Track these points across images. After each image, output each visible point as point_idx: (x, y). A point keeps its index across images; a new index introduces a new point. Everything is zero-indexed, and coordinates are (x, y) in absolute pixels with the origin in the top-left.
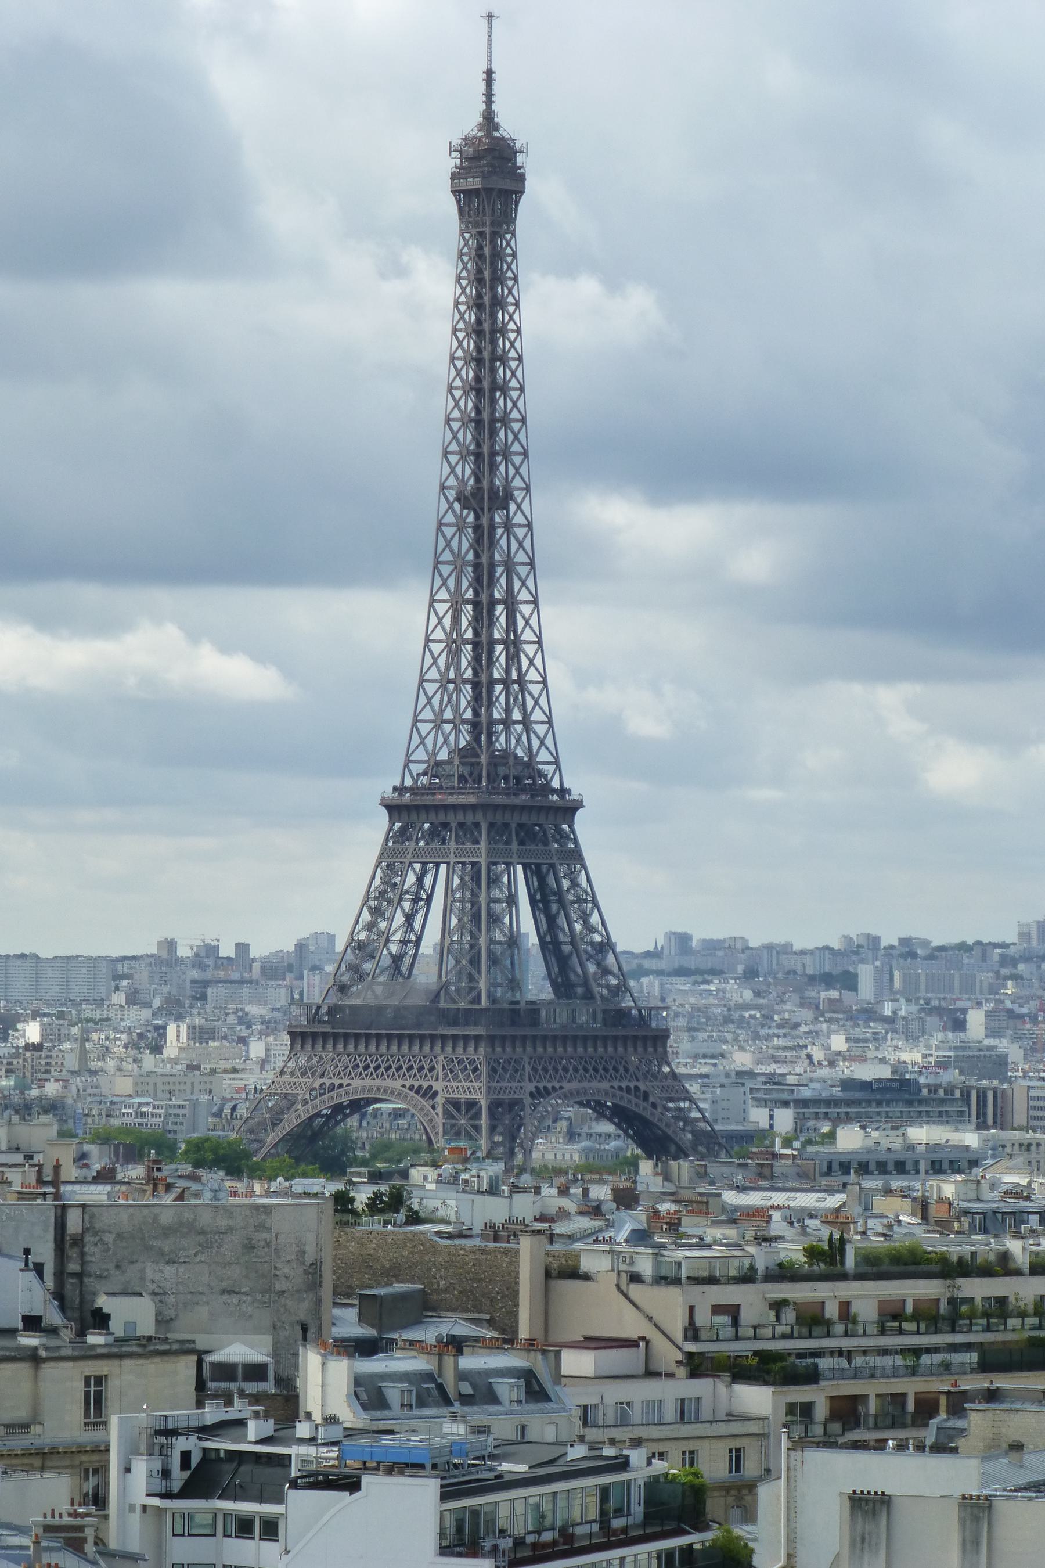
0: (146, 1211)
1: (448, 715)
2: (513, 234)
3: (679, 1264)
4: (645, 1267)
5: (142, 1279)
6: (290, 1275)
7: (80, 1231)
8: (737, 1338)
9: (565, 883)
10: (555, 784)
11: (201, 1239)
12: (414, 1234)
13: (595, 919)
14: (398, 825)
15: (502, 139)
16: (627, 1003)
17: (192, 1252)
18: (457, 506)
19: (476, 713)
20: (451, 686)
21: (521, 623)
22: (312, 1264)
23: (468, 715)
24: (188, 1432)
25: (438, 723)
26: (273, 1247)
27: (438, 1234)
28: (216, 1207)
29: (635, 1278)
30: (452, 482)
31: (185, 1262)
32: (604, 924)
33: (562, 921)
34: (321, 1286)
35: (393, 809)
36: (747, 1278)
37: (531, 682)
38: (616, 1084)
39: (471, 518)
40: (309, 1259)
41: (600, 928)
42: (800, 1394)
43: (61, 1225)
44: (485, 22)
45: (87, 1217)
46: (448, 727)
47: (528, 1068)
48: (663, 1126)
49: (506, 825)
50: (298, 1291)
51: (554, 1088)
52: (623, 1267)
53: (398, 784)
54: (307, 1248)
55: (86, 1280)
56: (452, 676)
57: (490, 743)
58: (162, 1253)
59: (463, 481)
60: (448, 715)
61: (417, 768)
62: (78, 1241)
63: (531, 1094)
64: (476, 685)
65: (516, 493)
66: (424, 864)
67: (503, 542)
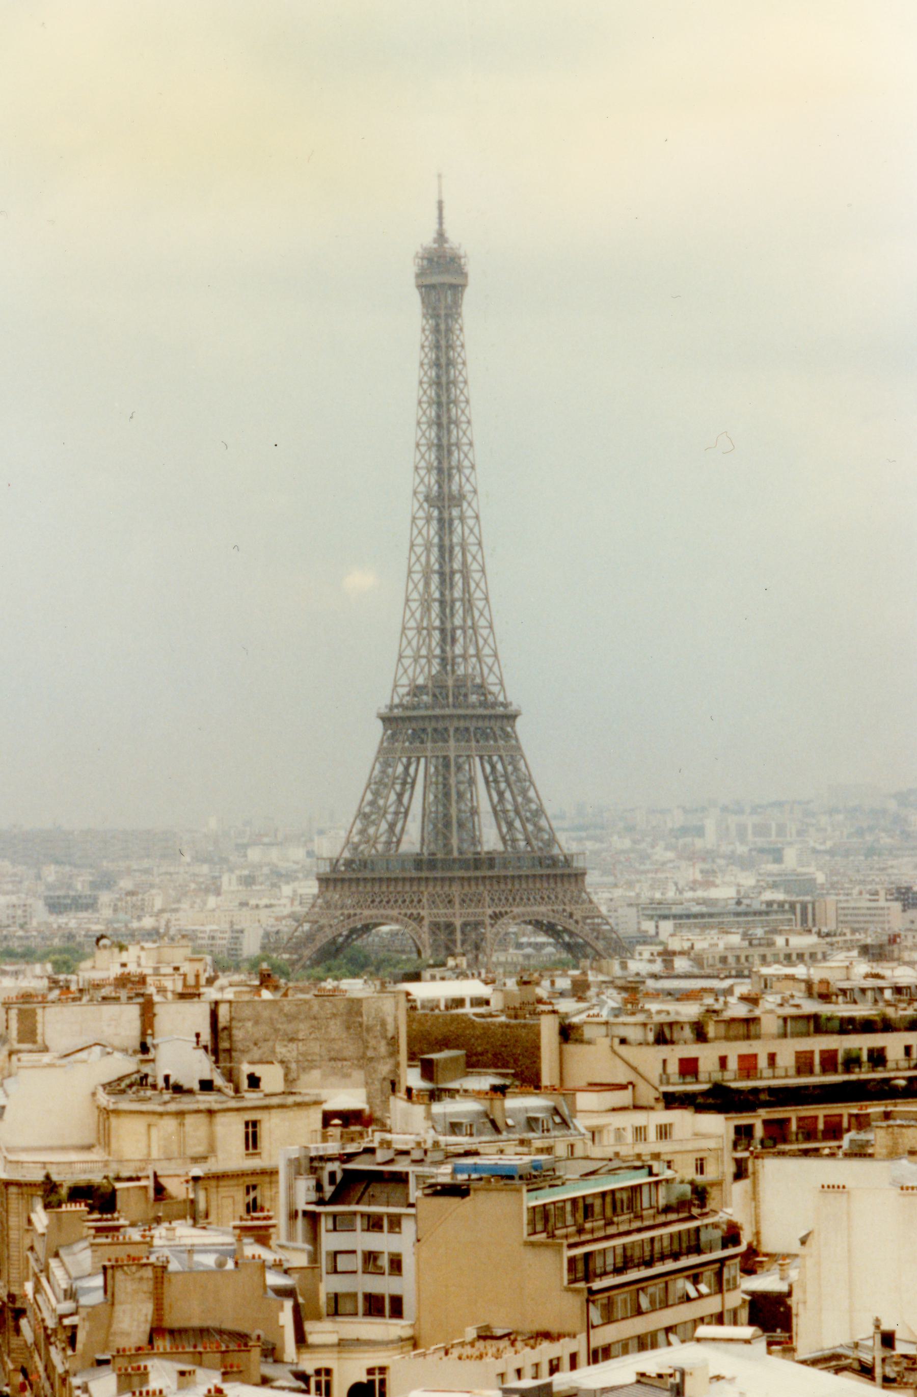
2: (459, 315)
5: (273, 1052)
8: (774, 1077)
9: (510, 768)
11: (314, 1022)
12: (458, 1015)
13: (531, 794)
14: (389, 732)
16: (555, 851)
18: (426, 505)
20: (425, 632)
23: (437, 651)
27: (476, 1015)
29: (623, 1041)
30: (422, 488)
33: (508, 795)
35: (387, 720)
37: (482, 627)
38: (550, 907)
39: (436, 513)
40: (390, 1035)
41: (536, 799)
42: (744, 1119)
43: (214, 1016)
46: (423, 661)
47: (488, 899)
49: (467, 729)
51: (506, 913)
53: (388, 702)
55: (234, 1054)
56: (425, 624)
57: (453, 671)
59: (429, 487)
60: (424, 652)
61: (403, 691)
63: (491, 917)
66: (409, 758)
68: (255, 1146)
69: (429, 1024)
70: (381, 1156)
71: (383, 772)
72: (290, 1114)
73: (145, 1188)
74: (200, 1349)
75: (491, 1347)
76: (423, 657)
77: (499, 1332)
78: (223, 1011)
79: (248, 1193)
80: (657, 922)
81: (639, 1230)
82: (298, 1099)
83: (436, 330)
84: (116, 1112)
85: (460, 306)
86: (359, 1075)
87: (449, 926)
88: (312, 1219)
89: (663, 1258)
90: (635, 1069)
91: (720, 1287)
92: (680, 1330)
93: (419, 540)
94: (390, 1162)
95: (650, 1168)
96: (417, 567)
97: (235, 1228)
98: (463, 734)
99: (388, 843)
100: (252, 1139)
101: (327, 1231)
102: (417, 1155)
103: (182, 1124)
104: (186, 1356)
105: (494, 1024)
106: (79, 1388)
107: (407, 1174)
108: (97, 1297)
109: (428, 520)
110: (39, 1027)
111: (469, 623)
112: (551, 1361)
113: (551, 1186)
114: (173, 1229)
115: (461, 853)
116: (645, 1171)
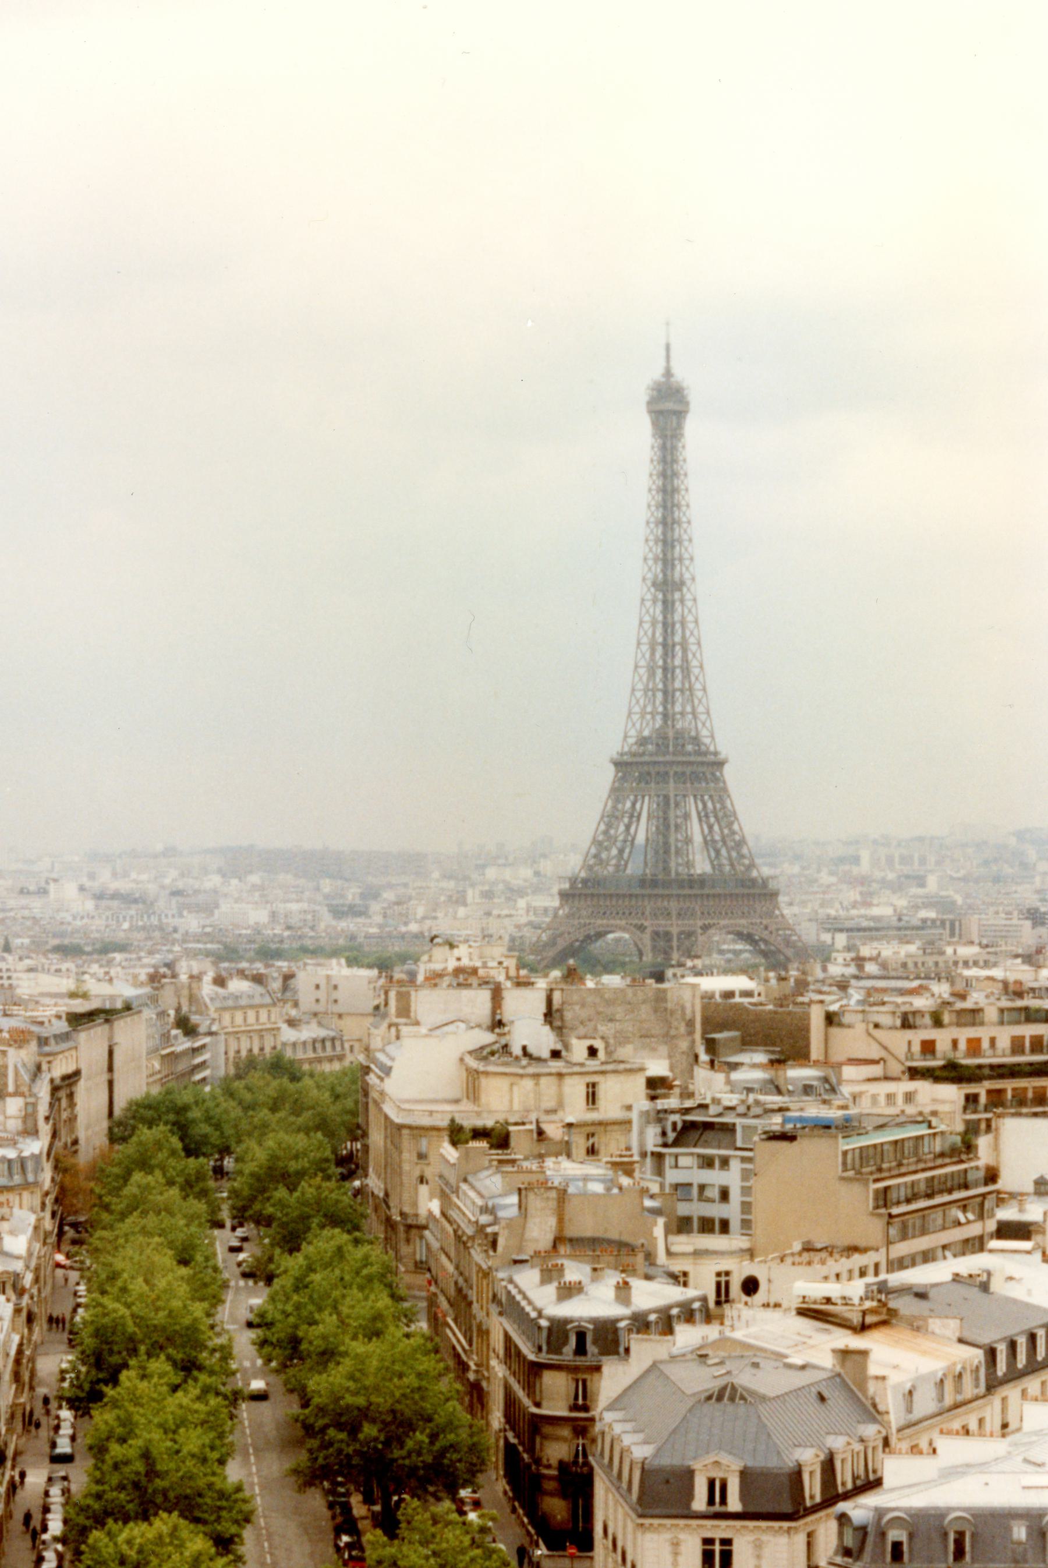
2: (682, 435)
5: (595, 1029)
9: (718, 806)
10: (712, 749)
13: (736, 827)
14: (620, 774)
18: (653, 590)
21: (690, 656)
23: (660, 709)
24: (673, 1112)
27: (751, 1004)
29: (876, 1026)
30: (650, 576)
32: (741, 829)
33: (716, 828)
35: (618, 764)
39: (660, 596)
40: (688, 1017)
46: (649, 717)
47: (699, 913)
53: (619, 749)
57: (673, 726)
59: (656, 576)
60: (649, 709)
61: (631, 741)
63: (701, 928)
64: (665, 692)
66: (636, 796)
68: (594, 1102)
70: (713, 1110)
71: (614, 807)
72: (622, 1078)
73: (531, 1131)
74: (598, 1253)
75: (816, 1257)
77: (819, 1246)
78: (557, 997)
79: (588, 1139)
81: (924, 1170)
82: (628, 1066)
83: (663, 448)
84: (487, 1074)
86: (664, 1049)
87: (667, 936)
88: (659, 1157)
89: (941, 1192)
90: (885, 1048)
91: (981, 1216)
92: (953, 1247)
93: (647, 618)
94: (720, 1115)
95: (930, 1122)
96: (645, 640)
97: (607, 1163)
98: (680, 777)
99: (617, 866)
100: (592, 1097)
101: (671, 1167)
102: (741, 1109)
103: (537, 1084)
104: (586, 1258)
106: (503, 1280)
107: (734, 1125)
108: (513, 1212)
109: (655, 601)
110: (413, 1005)
111: (687, 686)
112: (860, 1269)
113: (859, 1134)
114: (559, 1163)
116: (925, 1125)
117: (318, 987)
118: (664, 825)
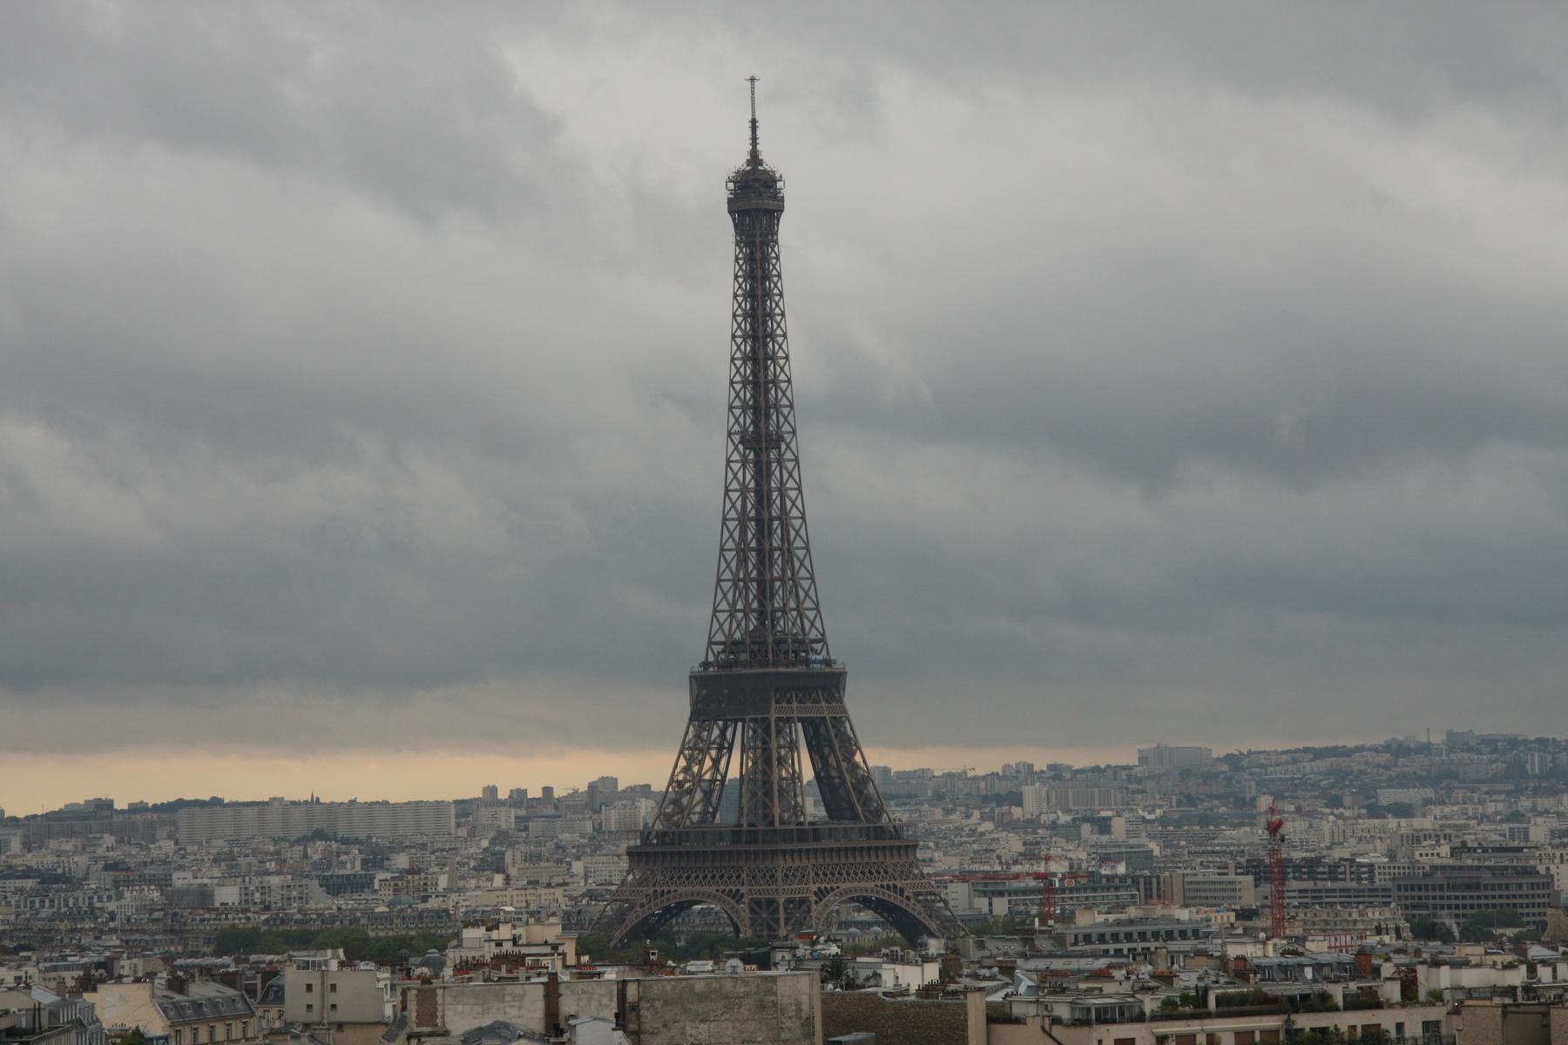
0: (684, 983)
1: (740, 606)
2: (776, 242)
3: (1089, 1010)
4: (1063, 1011)
5: (684, 1034)
6: (792, 1025)
7: (637, 999)
14: (704, 692)
15: (765, 170)
17: (719, 1012)
18: (741, 447)
19: (761, 604)
20: (741, 584)
21: (793, 534)
22: (807, 1019)
23: (755, 605)
25: (732, 612)
26: (779, 1007)
28: (736, 978)
29: (1057, 1021)
31: (714, 1020)
32: (864, 761)
33: (832, 760)
34: (814, 1035)
36: (1140, 1018)
38: (879, 883)
39: (751, 456)
40: (805, 1016)
41: (862, 765)
43: (622, 995)
44: (749, 84)
45: (641, 989)
46: (740, 615)
47: (812, 874)
48: (915, 914)
50: (798, 1039)
51: (832, 889)
52: (1045, 1013)
53: (703, 660)
54: (803, 1007)
55: (642, 1036)
56: (741, 576)
57: (773, 626)
58: (697, 1014)
59: (745, 429)
60: (740, 606)
61: (720, 648)
62: (635, 1008)
63: (815, 893)
64: (761, 583)
65: (786, 436)
66: (725, 722)
67: (777, 473)
69: (835, 1004)
71: (698, 736)
76: (739, 611)
78: (632, 991)
80: (990, 899)
83: (750, 259)
85: (776, 234)
87: (771, 903)
93: (735, 485)
96: (733, 514)
99: (704, 813)
105: (905, 1003)
109: (744, 462)
111: (789, 574)
115: (782, 822)
117: (309, 988)
118: (765, 760)
